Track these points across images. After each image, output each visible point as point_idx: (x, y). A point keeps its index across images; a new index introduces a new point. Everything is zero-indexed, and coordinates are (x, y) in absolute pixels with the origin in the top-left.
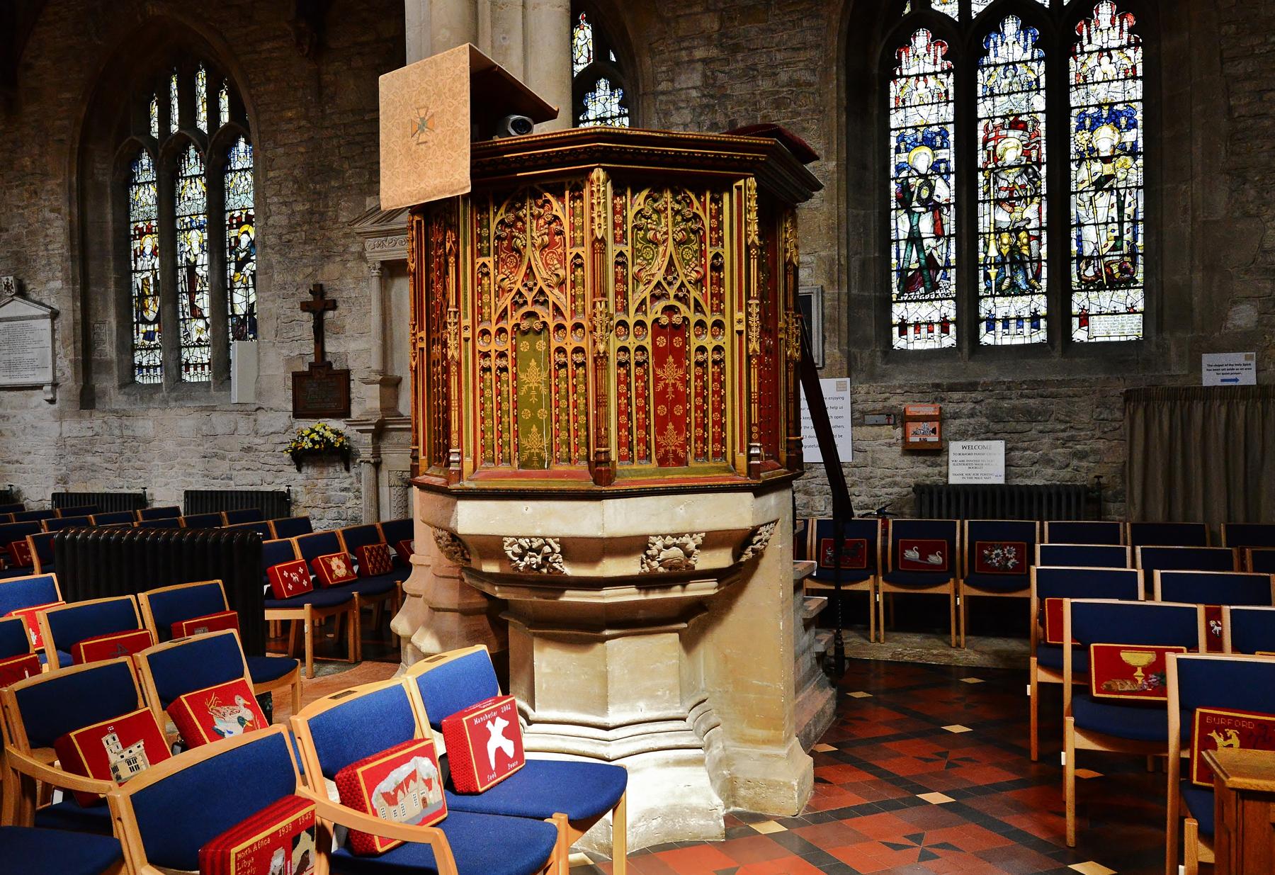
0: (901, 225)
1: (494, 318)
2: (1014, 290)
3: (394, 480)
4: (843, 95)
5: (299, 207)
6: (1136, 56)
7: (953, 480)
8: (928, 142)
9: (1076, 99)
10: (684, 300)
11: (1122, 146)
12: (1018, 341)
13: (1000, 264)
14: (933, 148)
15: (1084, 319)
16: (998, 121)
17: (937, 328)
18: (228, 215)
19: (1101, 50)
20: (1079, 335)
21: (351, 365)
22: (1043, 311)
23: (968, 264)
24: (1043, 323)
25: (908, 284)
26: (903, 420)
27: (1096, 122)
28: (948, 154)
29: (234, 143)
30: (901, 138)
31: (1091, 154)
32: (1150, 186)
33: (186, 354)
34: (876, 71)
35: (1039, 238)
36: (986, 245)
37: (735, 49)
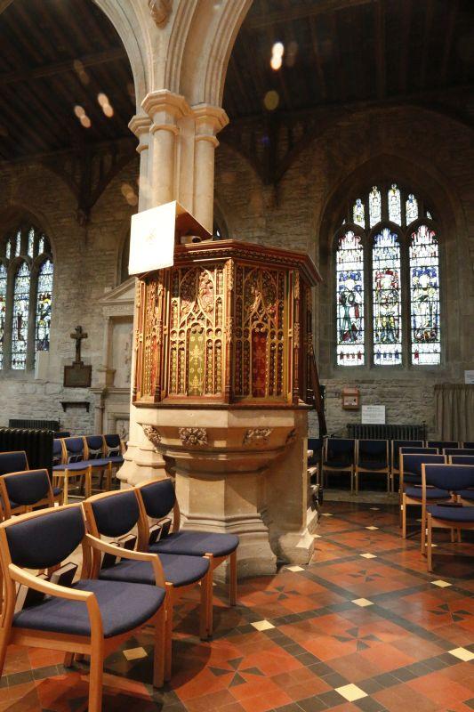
0: (341, 311)
1: (179, 326)
2: (388, 342)
3: (110, 417)
4: (318, 254)
5: (73, 291)
6: (435, 248)
7: (364, 422)
8: (353, 277)
9: (412, 263)
10: (266, 322)
11: (431, 284)
12: (390, 363)
13: (382, 330)
14: (355, 280)
15: (417, 355)
16: (381, 271)
17: (356, 356)
18: (39, 295)
19: (422, 245)
20: (415, 361)
21: (92, 363)
22: (400, 351)
23: (369, 330)
24: (400, 356)
25: (344, 337)
26: (343, 395)
27: (421, 273)
28: (361, 283)
29: (44, 262)
30: (342, 275)
31: (418, 287)
32: (441, 301)
33: (14, 357)
34: (331, 246)
35: (398, 320)
36: (377, 322)
37: (272, 233)
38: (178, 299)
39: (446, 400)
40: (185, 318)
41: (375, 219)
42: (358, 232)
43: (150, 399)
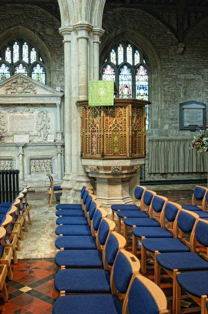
38: (108, 118)
39: (153, 146)
40: (111, 125)
41: (121, 61)
42: (112, 66)
43: (99, 156)
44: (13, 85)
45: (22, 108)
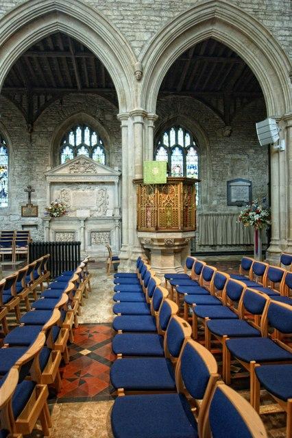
6: (197, 157)
9: (187, 163)
31: (190, 173)
40: (164, 201)
41: (173, 143)
43: (153, 229)
44: (76, 165)
45: (83, 186)
